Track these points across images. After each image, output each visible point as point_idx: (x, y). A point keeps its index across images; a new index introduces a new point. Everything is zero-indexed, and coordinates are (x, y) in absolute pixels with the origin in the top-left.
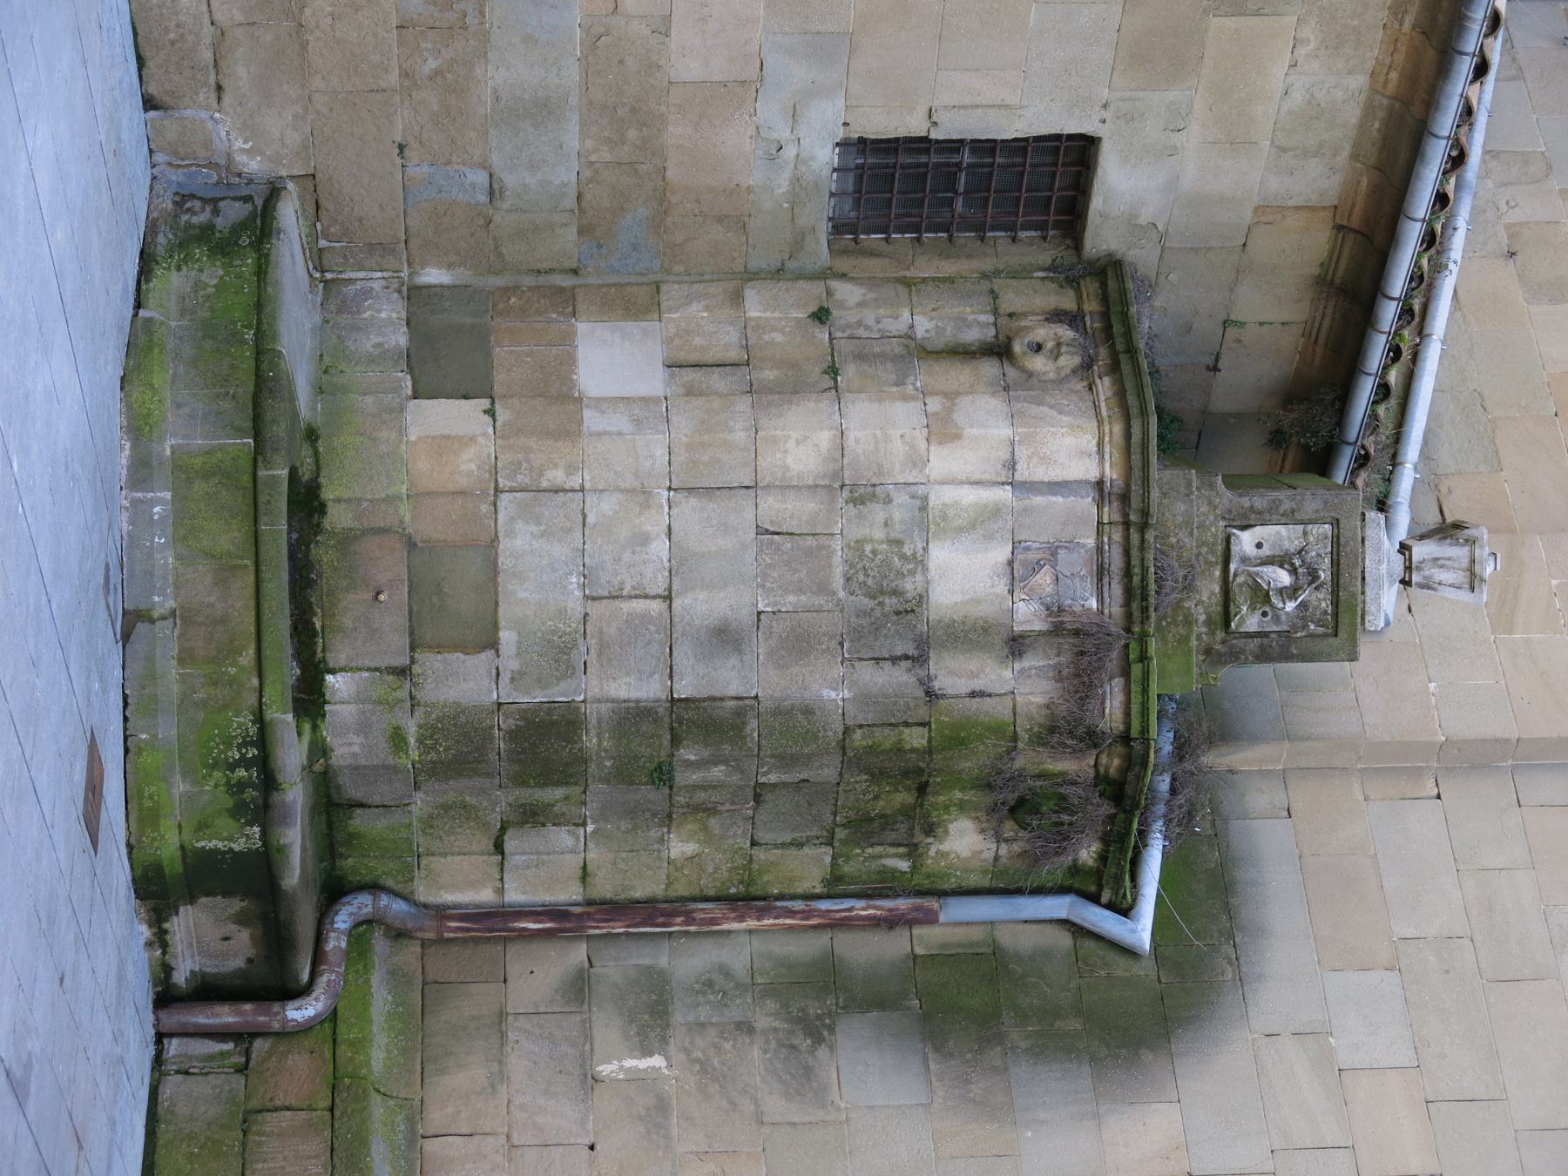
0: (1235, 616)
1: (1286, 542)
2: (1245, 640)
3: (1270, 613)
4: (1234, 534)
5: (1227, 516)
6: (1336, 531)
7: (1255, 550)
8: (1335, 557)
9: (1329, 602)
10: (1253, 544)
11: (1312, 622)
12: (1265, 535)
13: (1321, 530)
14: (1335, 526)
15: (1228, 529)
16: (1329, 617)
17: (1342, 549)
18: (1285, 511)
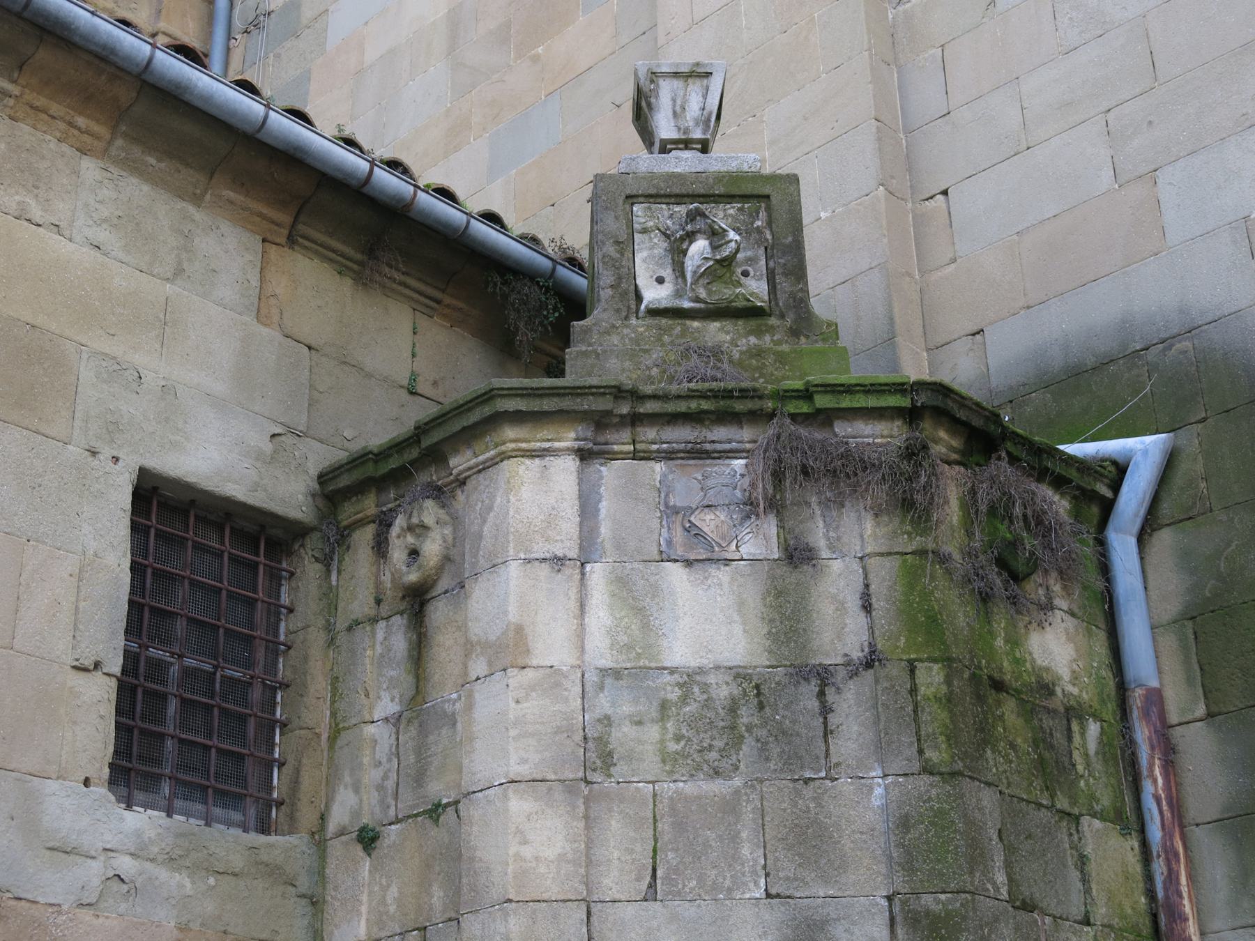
0: (749, 300)
1: (656, 251)
2: (778, 293)
3: (744, 268)
4: (646, 307)
5: (624, 314)
6: (641, 199)
7: (666, 284)
8: (673, 200)
9: (728, 206)
10: (659, 286)
11: (752, 224)
12: (648, 275)
13: (640, 213)
14: (635, 201)
15: (641, 315)
16: (746, 206)
17: (662, 192)
18: (618, 252)
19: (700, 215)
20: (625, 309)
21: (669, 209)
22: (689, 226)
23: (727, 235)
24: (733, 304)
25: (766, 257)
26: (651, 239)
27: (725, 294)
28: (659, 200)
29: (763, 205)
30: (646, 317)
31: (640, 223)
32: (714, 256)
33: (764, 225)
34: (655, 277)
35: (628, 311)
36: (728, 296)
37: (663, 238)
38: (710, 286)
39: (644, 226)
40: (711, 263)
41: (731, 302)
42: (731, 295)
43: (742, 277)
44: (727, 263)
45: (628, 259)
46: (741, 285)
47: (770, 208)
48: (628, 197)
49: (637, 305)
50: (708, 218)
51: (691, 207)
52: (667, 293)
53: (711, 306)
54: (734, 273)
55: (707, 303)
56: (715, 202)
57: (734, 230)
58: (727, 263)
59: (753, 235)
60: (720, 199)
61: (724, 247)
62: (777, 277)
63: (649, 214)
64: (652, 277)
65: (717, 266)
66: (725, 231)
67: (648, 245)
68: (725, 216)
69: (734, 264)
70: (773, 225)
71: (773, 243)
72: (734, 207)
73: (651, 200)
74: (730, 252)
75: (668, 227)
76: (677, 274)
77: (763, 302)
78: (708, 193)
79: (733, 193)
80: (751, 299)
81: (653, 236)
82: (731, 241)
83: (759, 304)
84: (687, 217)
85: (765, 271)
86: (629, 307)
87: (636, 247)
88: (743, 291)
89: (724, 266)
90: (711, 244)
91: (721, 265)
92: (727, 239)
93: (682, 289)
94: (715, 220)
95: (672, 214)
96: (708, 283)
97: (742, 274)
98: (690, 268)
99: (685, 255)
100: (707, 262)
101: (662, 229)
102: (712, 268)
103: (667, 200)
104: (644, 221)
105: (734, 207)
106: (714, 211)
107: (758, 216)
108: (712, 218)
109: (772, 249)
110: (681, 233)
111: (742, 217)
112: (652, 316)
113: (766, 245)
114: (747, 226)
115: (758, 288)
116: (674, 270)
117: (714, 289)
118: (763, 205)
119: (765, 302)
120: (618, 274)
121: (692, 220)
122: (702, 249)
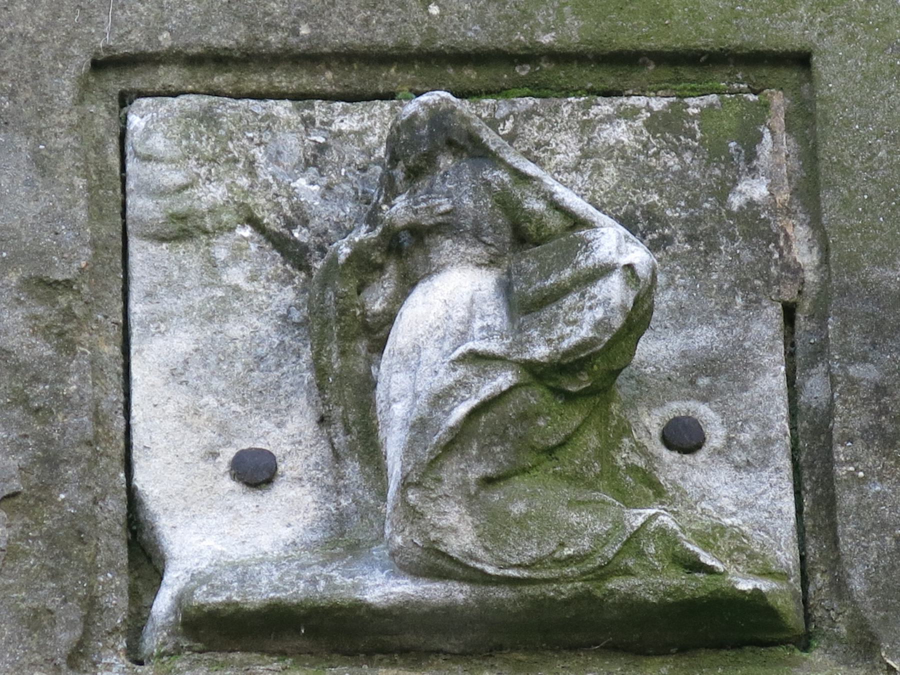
0: (694, 566)
1: (235, 329)
2: (847, 529)
3: (676, 408)
4: (180, 600)
5: (66, 637)
6: (169, 76)
7: (281, 490)
8: (327, 79)
9: (605, 107)
10: (247, 501)
11: (723, 191)
12: (193, 443)
13: (158, 143)
14: (138, 82)
15: (152, 642)
16: (694, 105)
17: (274, 39)
18: (45, 332)
19: (453, 146)
20: (74, 612)
21: (308, 122)
22: (400, 202)
23: (586, 244)
24: (613, 584)
25: (790, 356)
26: (212, 265)
27: (575, 532)
28: (258, 80)
29: (778, 100)
30: (178, 651)
31: (161, 192)
32: (520, 345)
33: (783, 196)
34: (229, 453)
35: (87, 621)
36: (586, 544)
37: (275, 263)
38: (496, 496)
39: (181, 206)
40: (504, 380)
41: (605, 572)
42: (600, 540)
43: (668, 456)
44: (584, 381)
45: (96, 366)
46: (659, 491)
47: (810, 116)
48: (99, 65)
49: (134, 595)
50: (490, 157)
51: (412, 107)
52: (287, 534)
53: (502, 594)
54: (625, 430)
55: (486, 579)
56: (538, 89)
57: (628, 222)
58: (584, 381)
59: (724, 244)
60: (562, 74)
61: (570, 300)
62: (841, 452)
63: (207, 147)
64: (215, 455)
65: (535, 397)
66: (576, 222)
67: (197, 299)
68: (586, 155)
69: (624, 387)
70: (827, 197)
71: (825, 283)
72: (633, 113)
73: (220, 80)
74: (598, 325)
75: (297, 208)
76: (340, 440)
77: (767, 573)
78: (502, 43)
79: (624, 41)
80: (707, 559)
81: (221, 254)
82: (604, 271)
83: (745, 585)
84: (394, 158)
85: (781, 425)
86: (91, 604)
87: (137, 308)
88: (667, 520)
89: (570, 398)
90: (506, 288)
91: (558, 392)
92: (585, 262)
93: (364, 511)
94: (530, 169)
95: (321, 148)
96: (488, 481)
97: (668, 441)
98: (399, 410)
99: (379, 346)
100: (482, 374)
101: (270, 219)
102: (511, 408)
103: (302, 80)
104: (178, 178)
105: (631, 114)
106: (532, 133)
107: (751, 156)
108: (512, 158)
109: (820, 316)
110: (362, 234)
111: (672, 161)
112: (210, 648)
113: (789, 293)
114: (692, 203)
115: (743, 505)
116: (322, 421)
117: (518, 508)
118: (778, 100)
119: (782, 576)
120: (45, 440)
121: (414, 174)
122: (461, 313)
